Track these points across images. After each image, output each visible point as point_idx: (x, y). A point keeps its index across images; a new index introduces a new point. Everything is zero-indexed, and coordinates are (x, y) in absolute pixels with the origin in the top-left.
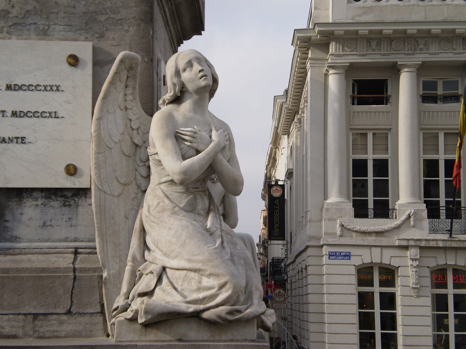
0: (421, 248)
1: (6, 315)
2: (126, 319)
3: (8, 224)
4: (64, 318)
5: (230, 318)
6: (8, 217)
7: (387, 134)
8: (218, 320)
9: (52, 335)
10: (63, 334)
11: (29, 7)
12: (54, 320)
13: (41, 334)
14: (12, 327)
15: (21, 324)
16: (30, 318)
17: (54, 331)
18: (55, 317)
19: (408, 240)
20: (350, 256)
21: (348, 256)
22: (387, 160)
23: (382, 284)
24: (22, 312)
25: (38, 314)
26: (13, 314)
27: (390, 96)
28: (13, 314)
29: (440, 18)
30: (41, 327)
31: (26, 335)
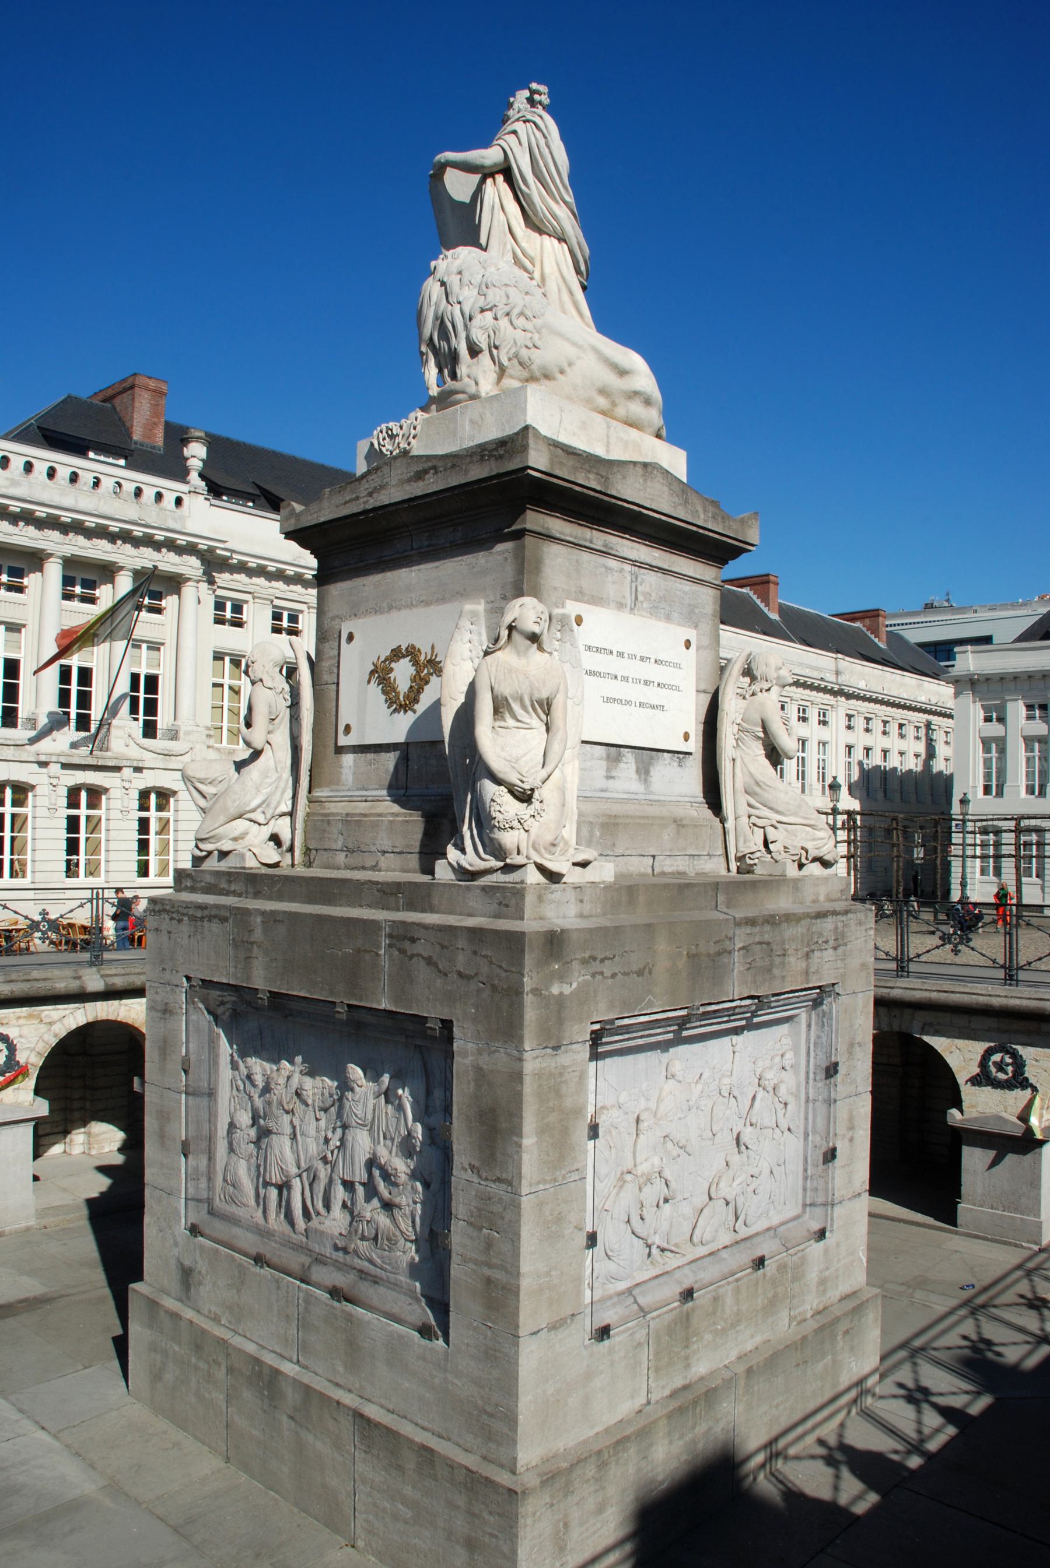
11: (661, 594)
23: (15, 804)
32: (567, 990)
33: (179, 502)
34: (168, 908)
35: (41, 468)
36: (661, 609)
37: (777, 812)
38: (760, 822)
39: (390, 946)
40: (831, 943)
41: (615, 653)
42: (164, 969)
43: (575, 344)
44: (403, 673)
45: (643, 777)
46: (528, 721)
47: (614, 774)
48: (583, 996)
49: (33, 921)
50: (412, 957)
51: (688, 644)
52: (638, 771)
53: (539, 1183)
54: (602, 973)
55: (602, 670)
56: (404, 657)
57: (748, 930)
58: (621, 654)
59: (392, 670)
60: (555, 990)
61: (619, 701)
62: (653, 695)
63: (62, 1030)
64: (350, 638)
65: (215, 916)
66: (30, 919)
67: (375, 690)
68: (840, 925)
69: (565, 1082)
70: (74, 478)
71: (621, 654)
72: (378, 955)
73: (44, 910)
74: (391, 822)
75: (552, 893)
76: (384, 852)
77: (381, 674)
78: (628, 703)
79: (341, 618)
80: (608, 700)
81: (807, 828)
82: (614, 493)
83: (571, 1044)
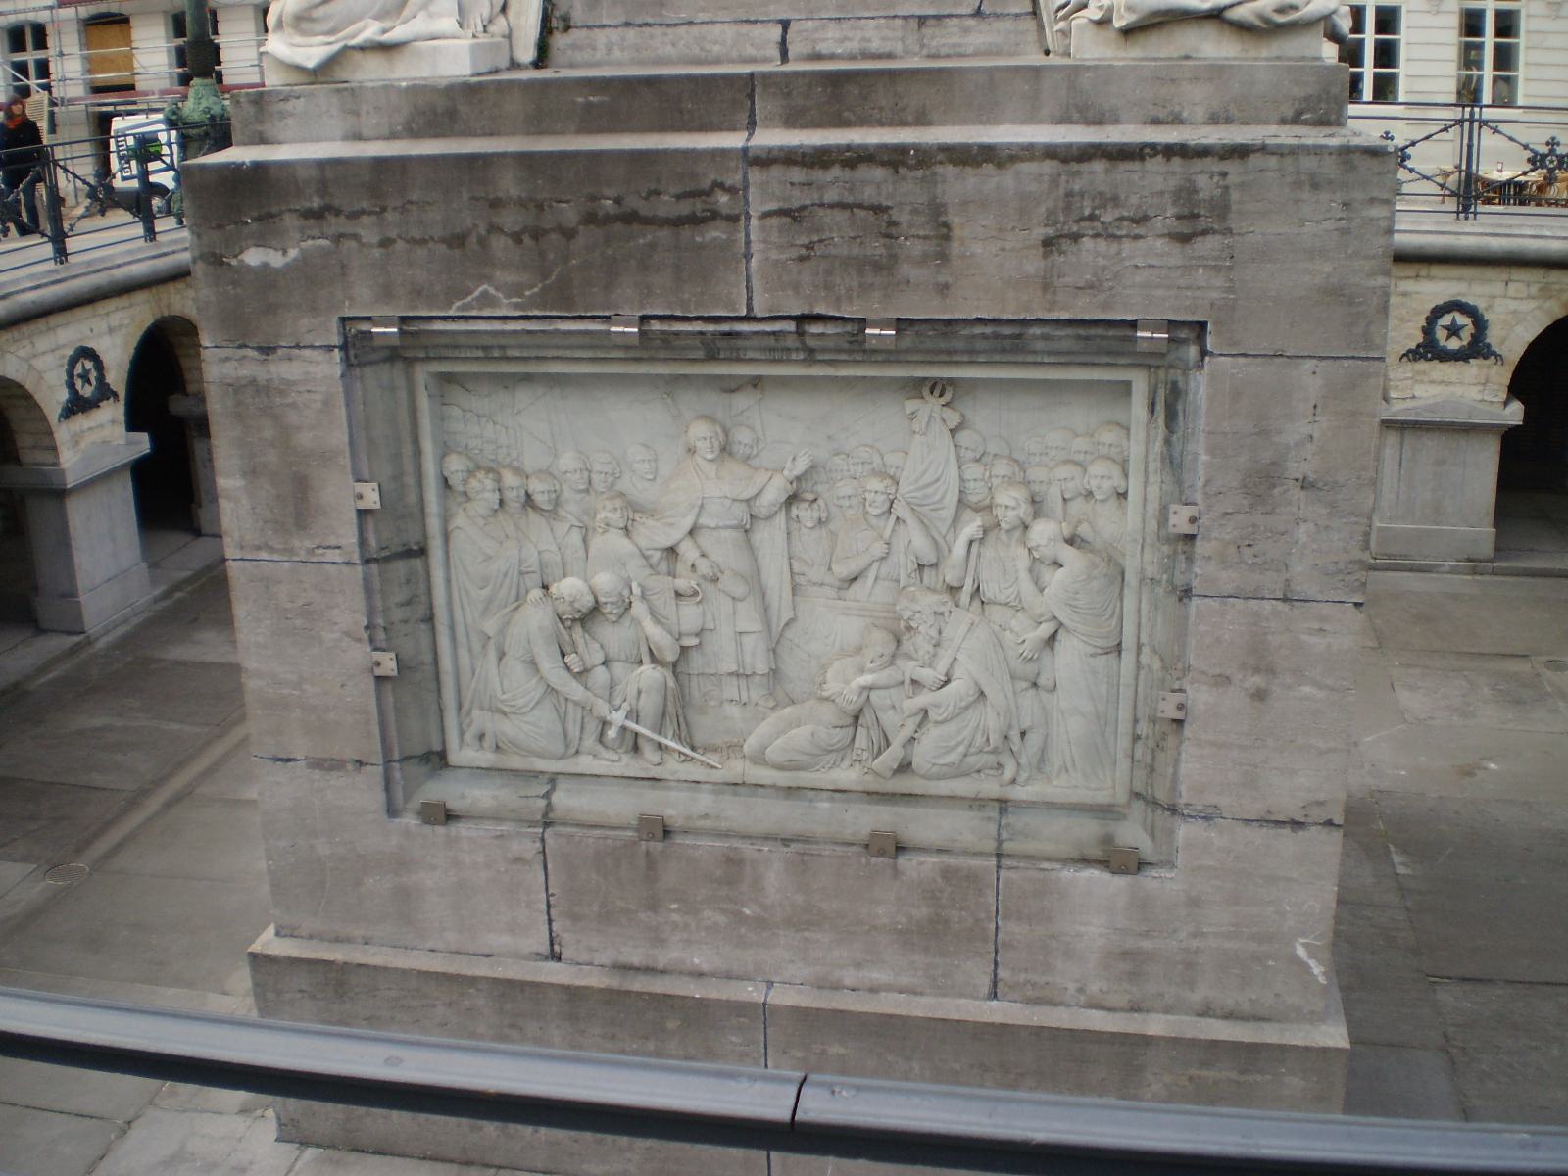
1: (873, 18)
2: (1090, 20)
4: (971, 22)
5: (1281, 19)
8: (1258, 22)
9: (951, 52)
10: (970, 50)
12: (955, 26)
13: (934, 51)
14: (884, 39)
15: (899, 34)
16: (914, 23)
17: (954, 46)
18: (955, 20)
24: (900, 13)
25: (926, 17)
26: (885, 17)
28: (885, 17)
30: (932, 38)
31: (907, 53)
32: (276, 259)
40: (1166, 219)
48: (305, 272)
53: (258, 548)
54: (355, 237)
57: (797, 174)
60: (253, 257)
68: (1202, 181)
69: (293, 405)
75: (286, 99)
83: (297, 346)
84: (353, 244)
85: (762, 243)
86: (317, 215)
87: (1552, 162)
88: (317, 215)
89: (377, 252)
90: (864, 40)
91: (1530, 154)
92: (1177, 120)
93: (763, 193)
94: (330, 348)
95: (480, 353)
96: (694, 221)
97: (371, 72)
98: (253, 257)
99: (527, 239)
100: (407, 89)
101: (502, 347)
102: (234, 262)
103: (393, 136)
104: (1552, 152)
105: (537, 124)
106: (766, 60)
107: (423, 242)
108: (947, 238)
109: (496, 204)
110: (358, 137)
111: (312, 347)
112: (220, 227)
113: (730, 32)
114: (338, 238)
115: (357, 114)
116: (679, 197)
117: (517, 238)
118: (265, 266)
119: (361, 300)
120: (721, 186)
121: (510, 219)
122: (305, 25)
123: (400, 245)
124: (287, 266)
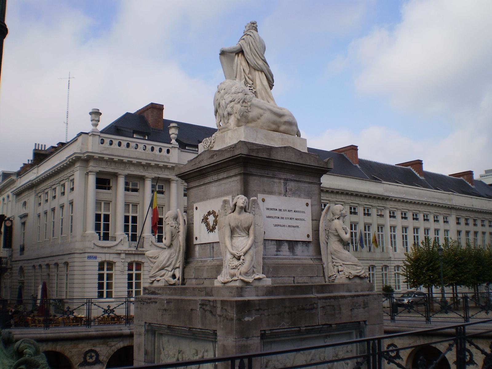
0: (126, 254)
3: (295, 251)
4: (316, 277)
6: (295, 249)
7: (163, 207)
11: (296, 188)
19: (121, 250)
20: (96, 258)
21: (96, 258)
22: (109, 215)
23: (108, 270)
27: (112, 187)
29: (135, 157)
32: (250, 319)
33: (168, 151)
34: (140, 300)
35: (116, 143)
36: (296, 193)
37: (343, 261)
38: (337, 264)
39: (201, 307)
40: (362, 306)
41: (278, 210)
42: (139, 321)
43: (262, 109)
44: (211, 219)
45: (291, 250)
46: (242, 234)
47: (280, 250)
49: (105, 310)
50: (206, 311)
51: (307, 205)
52: (289, 249)
54: (264, 314)
55: (273, 215)
56: (211, 214)
57: (324, 301)
58: (280, 210)
59: (208, 219)
60: (246, 319)
61: (281, 226)
62: (294, 223)
63: (115, 349)
64: (197, 208)
65: (153, 302)
66: (104, 309)
67: (204, 225)
68: (365, 300)
70: (128, 145)
71: (280, 210)
72: (197, 311)
73: (109, 306)
74: (207, 268)
75: (246, 288)
76: (205, 279)
77: (205, 220)
78: (284, 226)
79: (194, 202)
80: (276, 225)
81: (354, 266)
82: (273, 158)
83: (253, 337)
84: (263, 316)
85: (320, 312)
86: (258, 310)
87: (68, 313)
88: (258, 310)
89: (267, 317)
90: (304, 280)
91: (103, 310)
92: (358, 291)
93: (320, 304)
94: (258, 337)
95: (275, 337)
96: (312, 309)
97: (257, 284)
98: (246, 319)
99: (289, 313)
100: (266, 287)
101: (278, 335)
102: (243, 320)
103: (263, 296)
104: (68, 310)
105: (284, 294)
106: (292, 283)
107: (274, 315)
108: (341, 310)
109: (285, 307)
110: (257, 296)
111: (255, 337)
112: (241, 313)
113: (287, 278)
114: (261, 315)
115: (258, 291)
116: (310, 305)
117: (288, 313)
118: (249, 321)
119: (264, 327)
120: (315, 303)
121: (287, 310)
122: (247, 274)
123: (271, 315)
124: (252, 321)
